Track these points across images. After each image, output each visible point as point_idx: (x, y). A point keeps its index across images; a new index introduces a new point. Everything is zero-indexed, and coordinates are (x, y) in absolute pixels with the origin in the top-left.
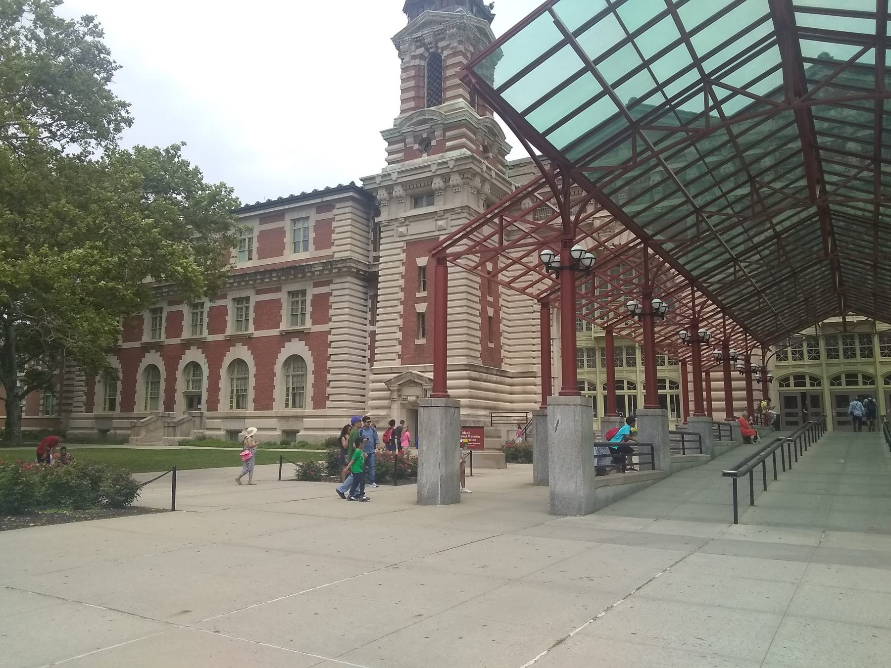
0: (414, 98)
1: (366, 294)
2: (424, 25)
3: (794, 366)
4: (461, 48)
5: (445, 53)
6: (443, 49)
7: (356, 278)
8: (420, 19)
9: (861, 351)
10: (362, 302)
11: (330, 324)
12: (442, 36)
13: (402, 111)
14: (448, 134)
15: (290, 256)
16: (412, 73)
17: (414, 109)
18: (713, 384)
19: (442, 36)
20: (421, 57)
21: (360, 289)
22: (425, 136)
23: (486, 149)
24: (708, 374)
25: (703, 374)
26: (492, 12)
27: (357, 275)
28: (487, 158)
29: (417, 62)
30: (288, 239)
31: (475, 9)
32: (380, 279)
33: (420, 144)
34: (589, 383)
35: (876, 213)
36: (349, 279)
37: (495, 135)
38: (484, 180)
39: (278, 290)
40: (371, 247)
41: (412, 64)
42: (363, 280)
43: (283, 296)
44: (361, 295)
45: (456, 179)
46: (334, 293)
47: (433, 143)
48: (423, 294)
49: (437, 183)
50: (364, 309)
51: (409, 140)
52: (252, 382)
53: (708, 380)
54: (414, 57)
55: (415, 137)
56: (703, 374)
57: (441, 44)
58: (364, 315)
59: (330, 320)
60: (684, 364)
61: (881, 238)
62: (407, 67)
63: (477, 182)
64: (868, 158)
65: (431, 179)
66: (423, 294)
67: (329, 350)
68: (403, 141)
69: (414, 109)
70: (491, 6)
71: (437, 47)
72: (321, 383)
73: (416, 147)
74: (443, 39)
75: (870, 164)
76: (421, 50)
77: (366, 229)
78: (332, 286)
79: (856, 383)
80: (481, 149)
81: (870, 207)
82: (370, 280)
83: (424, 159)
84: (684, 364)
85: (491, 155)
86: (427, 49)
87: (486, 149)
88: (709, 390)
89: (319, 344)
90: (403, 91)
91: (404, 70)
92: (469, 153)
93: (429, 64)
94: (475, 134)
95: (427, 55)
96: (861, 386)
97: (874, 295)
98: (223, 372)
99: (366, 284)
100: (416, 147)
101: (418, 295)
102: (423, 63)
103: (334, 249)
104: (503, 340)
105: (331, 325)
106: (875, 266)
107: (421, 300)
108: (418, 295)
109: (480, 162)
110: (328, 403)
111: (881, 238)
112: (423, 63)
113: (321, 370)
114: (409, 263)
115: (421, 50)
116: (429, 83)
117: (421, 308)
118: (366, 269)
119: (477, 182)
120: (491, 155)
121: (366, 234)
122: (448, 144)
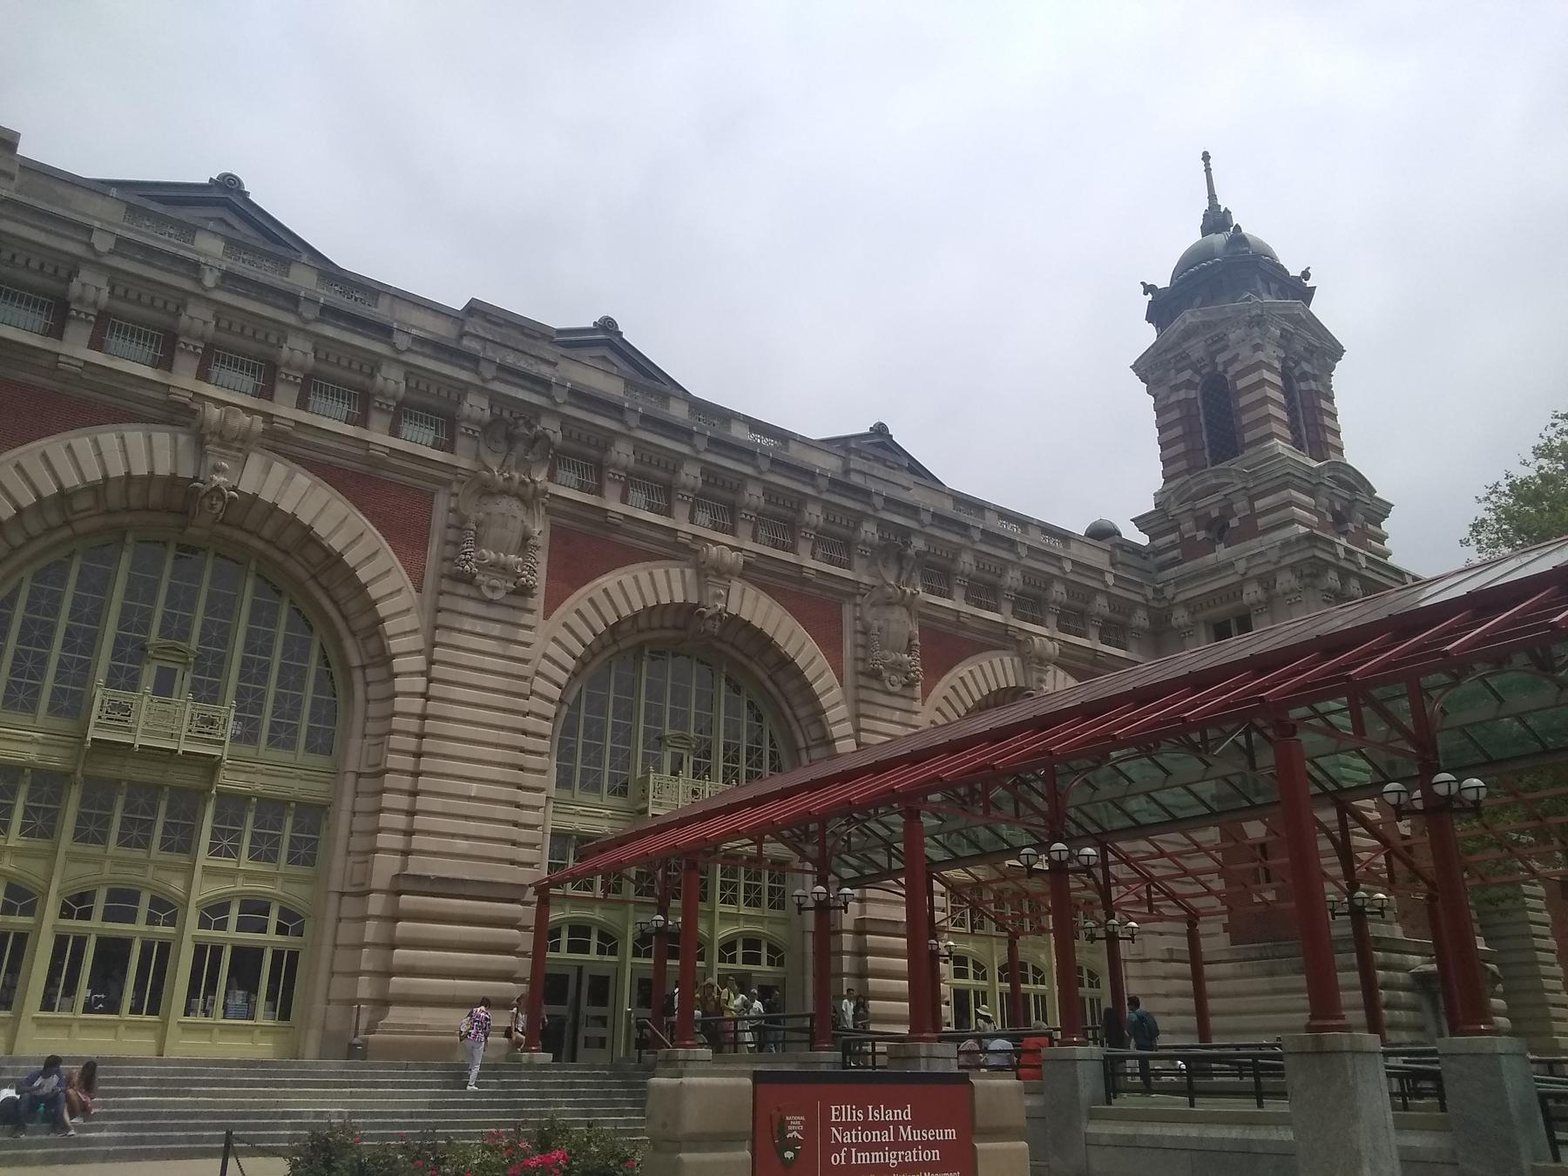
0: (1185, 454)
2: (1187, 334)
3: (748, 919)
4: (1261, 356)
5: (1231, 371)
6: (1227, 364)
8: (1178, 325)
12: (1218, 346)
13: (1167, 478)
14: (1259, 504)
16: (1175, 415)
17: (1188, 471)
19: (1218, 346)
20: (1189, 384)
22: (1215, 514)
23: (1340, 520)
26: (1309, 284)
28: (1345, 533)
29: (1182, 395)
31: (1273, 286)
33: (1208, 529)
37: (1351, 488)
38: (1345, 575)
41: (1173, 398)
45: (1286, 581)
47: (1234, 523)
49: (1252, 593)
51: (1187, 525)
54: (1176, 388)
55: (1197, 520)
57: (1220, 359)
60: (1192, 918)
62: (1166, 407)
63: (1332, 579)
65: (1235, 591)
68: (1175, 528)
69: (1188, 471)
70: (1306, 275)
71: (1215, 365)
73: (1201, 535)
76: (1187, 374)
79: (585, 949)
80: (1330, 518)
83: (1222, 553)
84: (1192, 918)
85: (1351, 526)
86: (1197, 371)
87: (1340, 520)
90: (1164, 445)
91: (1160, 410)
92: (1303, 530)
93: (1204, 396)
94: (1311, 494)
95: (1197, 379)
96: (593, 956)
100: (1201, 535)
102: (1193, 394)
109: (1332, 544)
112: (1193, 394)
115: (1187, 374)
116: (1208, 423)
119: (1332, 579)
120: (1351, 526)
122: (1261, 522)
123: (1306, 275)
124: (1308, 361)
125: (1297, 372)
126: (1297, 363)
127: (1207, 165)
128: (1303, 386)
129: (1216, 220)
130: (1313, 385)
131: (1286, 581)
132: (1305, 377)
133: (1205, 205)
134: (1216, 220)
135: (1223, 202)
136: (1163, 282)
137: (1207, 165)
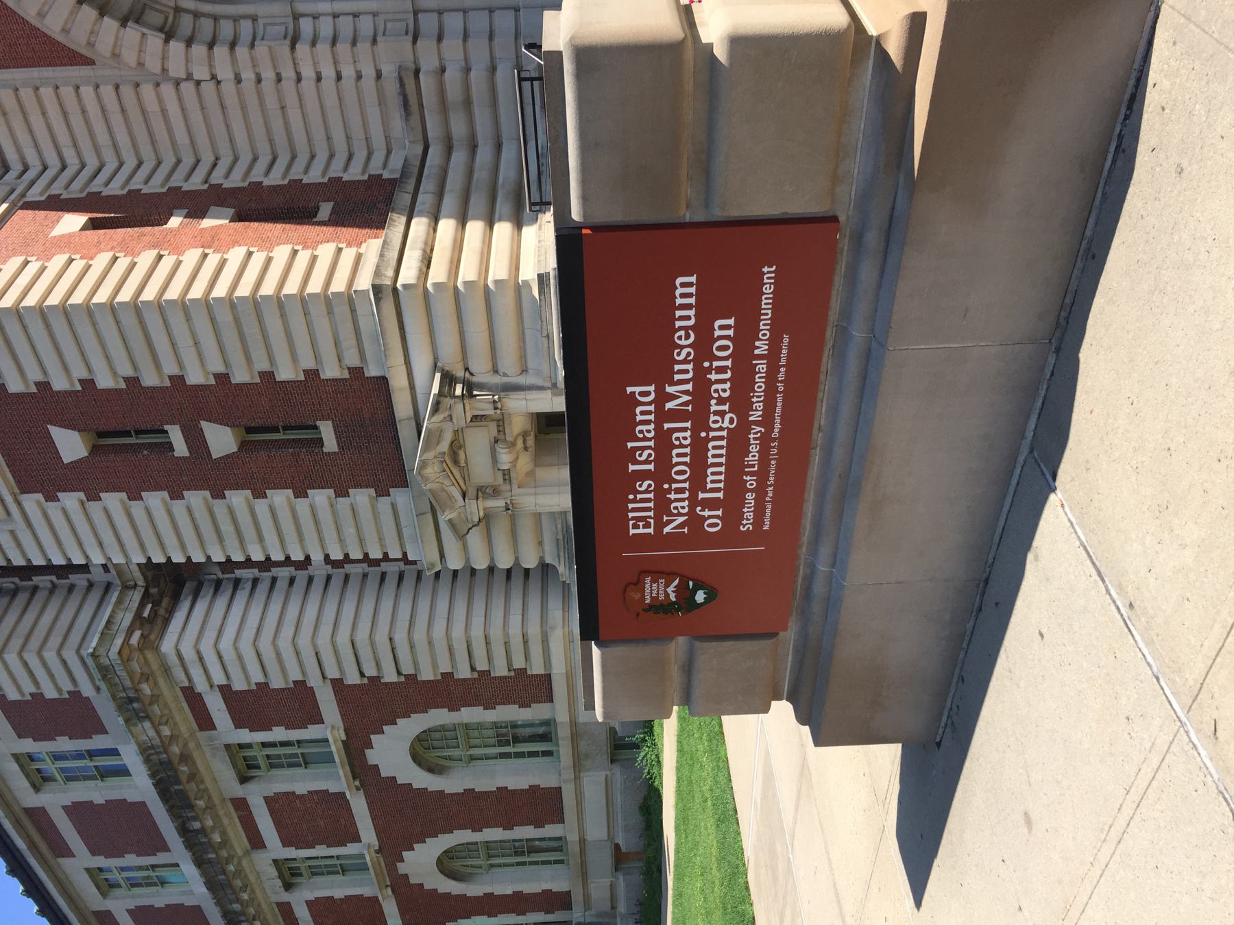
1: (218, 584)
7: (167, 621)
10: (242, 596)
11: (311, 683)
15: (139, 786)
21: (201, 606)
27: (152, 622)
30: (96, 793)
32: (158, 558)
36: (167, 646)
39: (241, 805)
40: (79, 580)
42: (176, 599)
43: (256, 795)
44: (221, 602)
46: (219, 679)
48: (176, 436)
50: (263, 587)
52: (494, 834)
58: (282, 585)
59: (301, 684)
66: (176, 436)
67: (386, 679)
72: (483, 689)
77: (22, 598)
78: (201, 686)
82: (171, 584)
89: (370, 704)
98: (473, 890)
99: (189, 586)
101: (180, 448)
103: (87, 690)
104: (315, 176)
105: (314, 681)
107: (196, 440)
108: (180, 448)
110: (537, 669)
113: (447, 691)
114: (86, 480)
117: (221, 440)
118: (137, 596)
121: (40, 597)
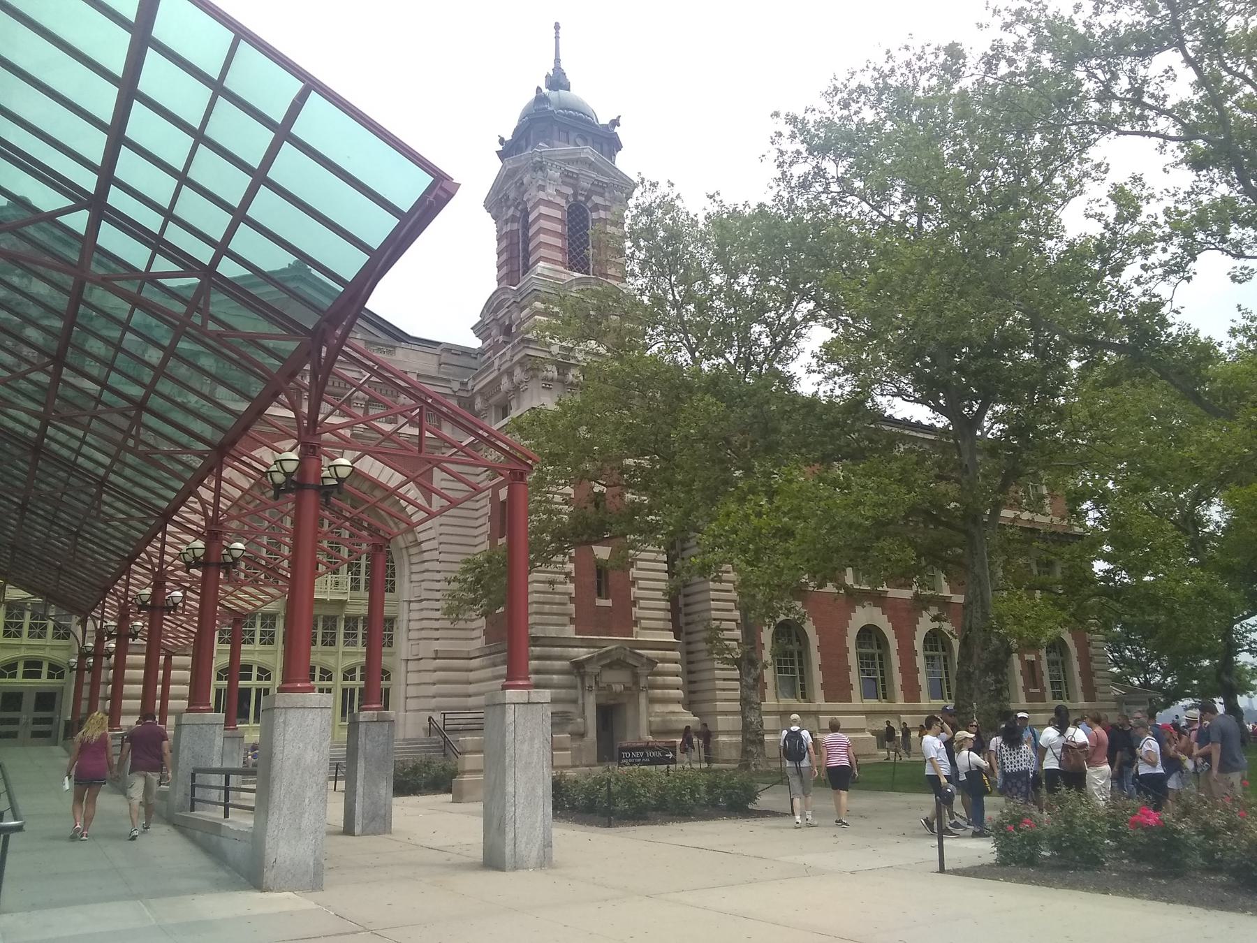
9: (30, 627)
18: (175, 674)
24: (168, 659)
25: (162, 658)
34: (260, 669)
35: (42, 433)
47: (514, 330)
53: (168, 667)
56: (162, 658)
61: (40, 470)
64: (48, 355)
74: (526, 191)
75: (48, 364)
81: (36, 423)
88: (166, 682)
97: (13, 547)
106: (22, 508)
111: (40, 470)
123: (615, 123)
124: (602, 195)
125: (589, 205)
126: (588, 198)
127: (557, 33)
128: (594, 216)
129: (557, 81)
130: (602, 214)
131: (519, 374)
132: (596, 207)
133: (549, 68)
134: (557, 81)
135: (563, 66)
136: (508, 137)
137: (557, 33)
